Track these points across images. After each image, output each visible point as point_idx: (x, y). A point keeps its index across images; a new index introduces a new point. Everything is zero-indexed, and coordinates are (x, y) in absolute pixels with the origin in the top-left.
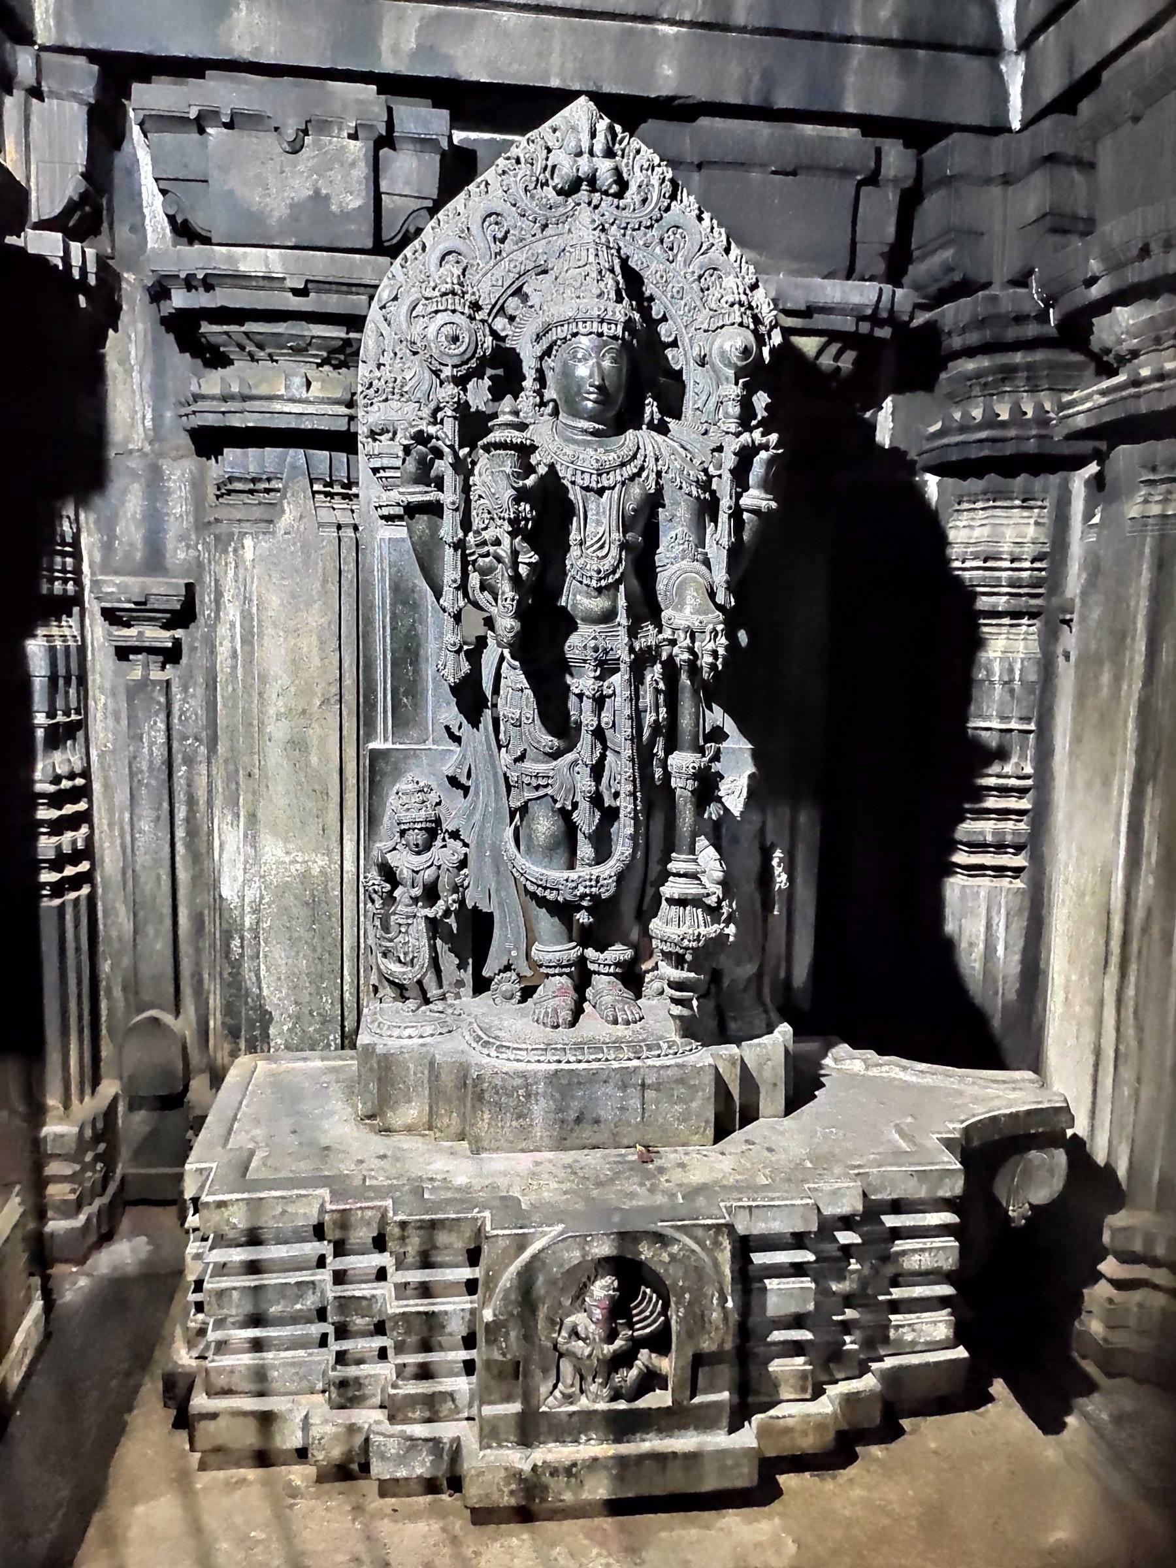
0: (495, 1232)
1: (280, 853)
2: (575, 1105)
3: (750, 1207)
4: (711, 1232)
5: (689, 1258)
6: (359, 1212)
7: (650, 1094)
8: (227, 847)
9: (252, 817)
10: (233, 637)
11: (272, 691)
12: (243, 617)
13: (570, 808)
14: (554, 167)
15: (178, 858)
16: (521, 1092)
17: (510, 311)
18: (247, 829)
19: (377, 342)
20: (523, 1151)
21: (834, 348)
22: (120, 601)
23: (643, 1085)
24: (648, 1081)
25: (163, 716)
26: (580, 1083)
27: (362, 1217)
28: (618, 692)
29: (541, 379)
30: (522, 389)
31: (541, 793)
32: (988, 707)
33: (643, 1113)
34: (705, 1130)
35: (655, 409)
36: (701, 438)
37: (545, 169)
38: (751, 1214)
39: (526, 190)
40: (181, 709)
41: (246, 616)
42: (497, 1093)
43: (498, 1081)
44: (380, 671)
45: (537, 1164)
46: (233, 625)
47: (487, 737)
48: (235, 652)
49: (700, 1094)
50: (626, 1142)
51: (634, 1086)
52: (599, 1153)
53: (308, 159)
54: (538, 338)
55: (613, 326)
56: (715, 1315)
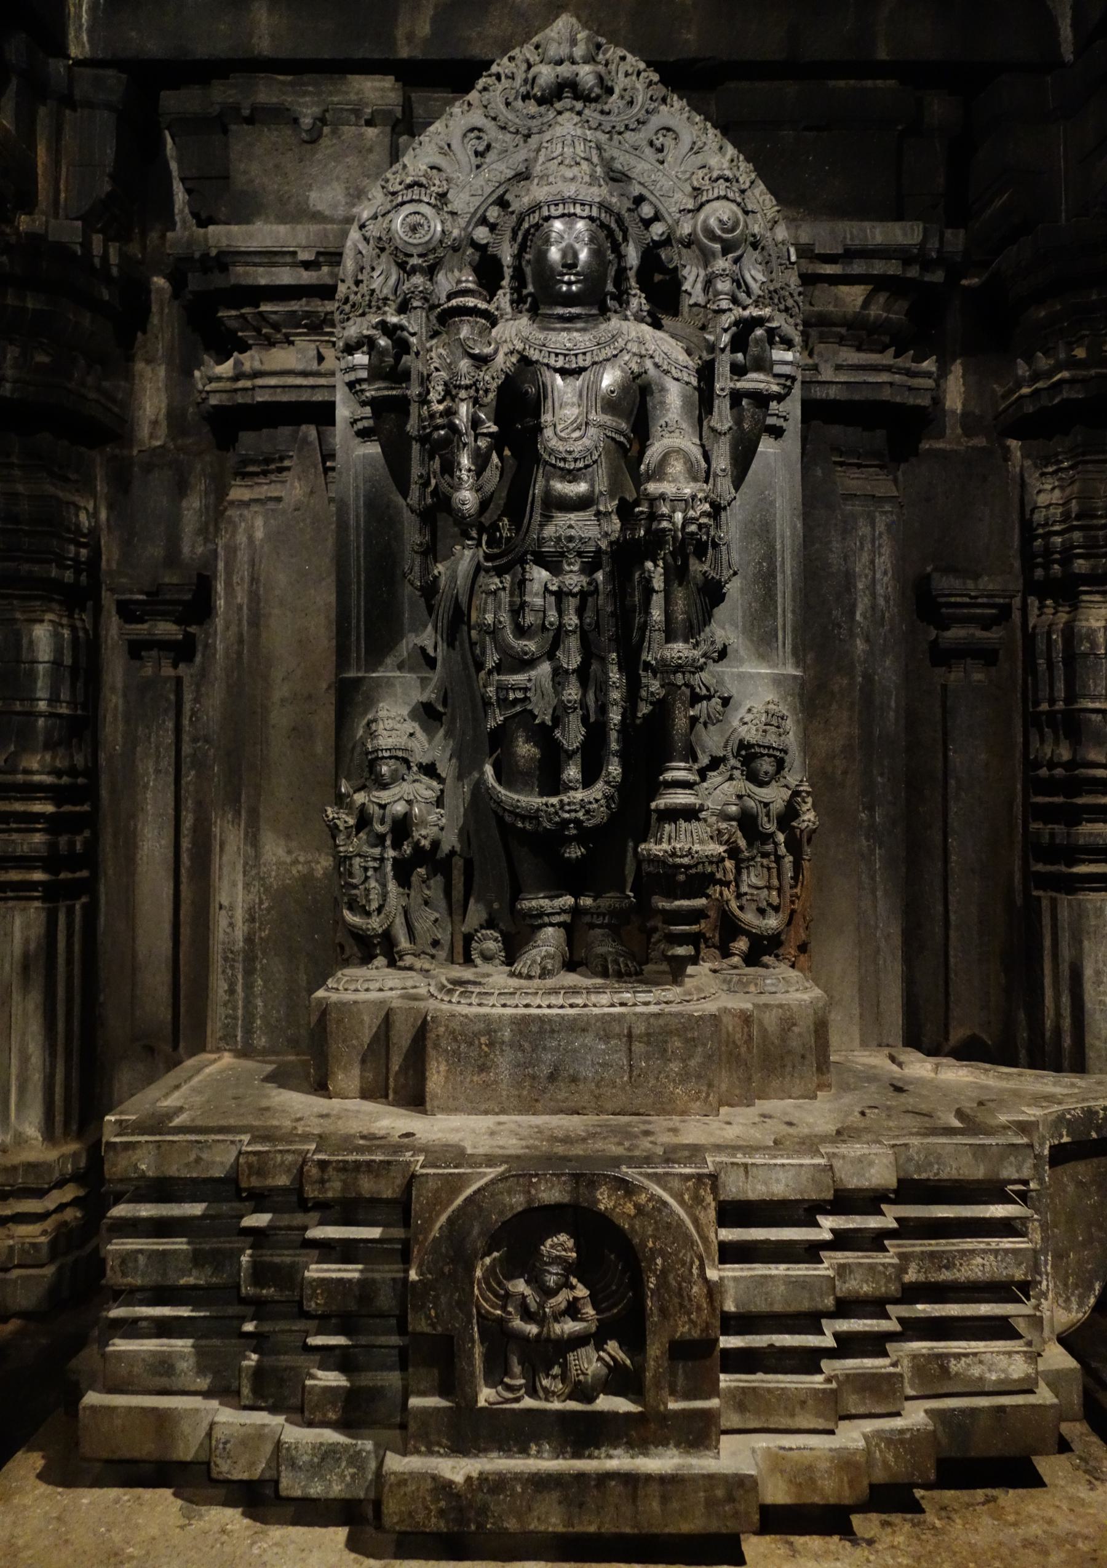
0: (424, 1171)
1: (281, 852)
2: (548, 1057)
3: (746, 1165)
4: (690, 1183)
5: (660, 1211)
6: (279, 1157)
7: (638, 1047)
8: (227, 848)
9: (254, 814)
10: (240, 624)
11: (278, 674)
12: (250, 601)
13: (550, 723)
14: (534, 79)
15: (183, 871)
16: (483, 1040)
17: (492, 220)
18: (247, 826)
19: (355, 258)
20: (486, 1112)
21: (882, 298)
22: (132, 592)
23: (630, 1036)
24: (636, 1031)
25: (172, 714)
26: (553, 1031)
27: (283, 1162)
28: (601, 587)
29: (519, 275)
30: (501, 287)
31: (518, 709)
32: (1096, 686)
33: (631, 1071)
34: (708, 1095)
35: (644, 301)
36: (699, 333)
37: (526, 81)
38: (747, 1172)
39: (508, 104)
40: (192, 709)
41: (254, 597)
42: (455, 1039)
43: (455, 1025)
44: (354, 595)
45: (500, 1123)
46: (240, 607)
47: (463, 657)
48: (241, 635)
49: (700, 1049)
50: (609, 1106)
51: (619, 1036)
52: (576, 1118)
53: (326, 147)
54: (515, 233)
55: (587, 208)
56: (695, 1289)
